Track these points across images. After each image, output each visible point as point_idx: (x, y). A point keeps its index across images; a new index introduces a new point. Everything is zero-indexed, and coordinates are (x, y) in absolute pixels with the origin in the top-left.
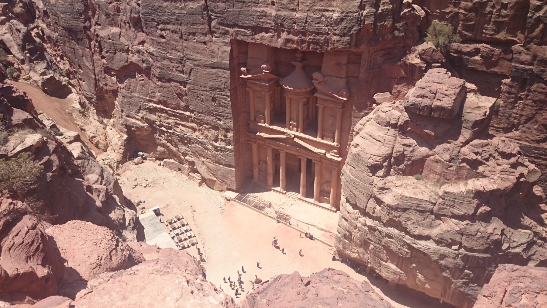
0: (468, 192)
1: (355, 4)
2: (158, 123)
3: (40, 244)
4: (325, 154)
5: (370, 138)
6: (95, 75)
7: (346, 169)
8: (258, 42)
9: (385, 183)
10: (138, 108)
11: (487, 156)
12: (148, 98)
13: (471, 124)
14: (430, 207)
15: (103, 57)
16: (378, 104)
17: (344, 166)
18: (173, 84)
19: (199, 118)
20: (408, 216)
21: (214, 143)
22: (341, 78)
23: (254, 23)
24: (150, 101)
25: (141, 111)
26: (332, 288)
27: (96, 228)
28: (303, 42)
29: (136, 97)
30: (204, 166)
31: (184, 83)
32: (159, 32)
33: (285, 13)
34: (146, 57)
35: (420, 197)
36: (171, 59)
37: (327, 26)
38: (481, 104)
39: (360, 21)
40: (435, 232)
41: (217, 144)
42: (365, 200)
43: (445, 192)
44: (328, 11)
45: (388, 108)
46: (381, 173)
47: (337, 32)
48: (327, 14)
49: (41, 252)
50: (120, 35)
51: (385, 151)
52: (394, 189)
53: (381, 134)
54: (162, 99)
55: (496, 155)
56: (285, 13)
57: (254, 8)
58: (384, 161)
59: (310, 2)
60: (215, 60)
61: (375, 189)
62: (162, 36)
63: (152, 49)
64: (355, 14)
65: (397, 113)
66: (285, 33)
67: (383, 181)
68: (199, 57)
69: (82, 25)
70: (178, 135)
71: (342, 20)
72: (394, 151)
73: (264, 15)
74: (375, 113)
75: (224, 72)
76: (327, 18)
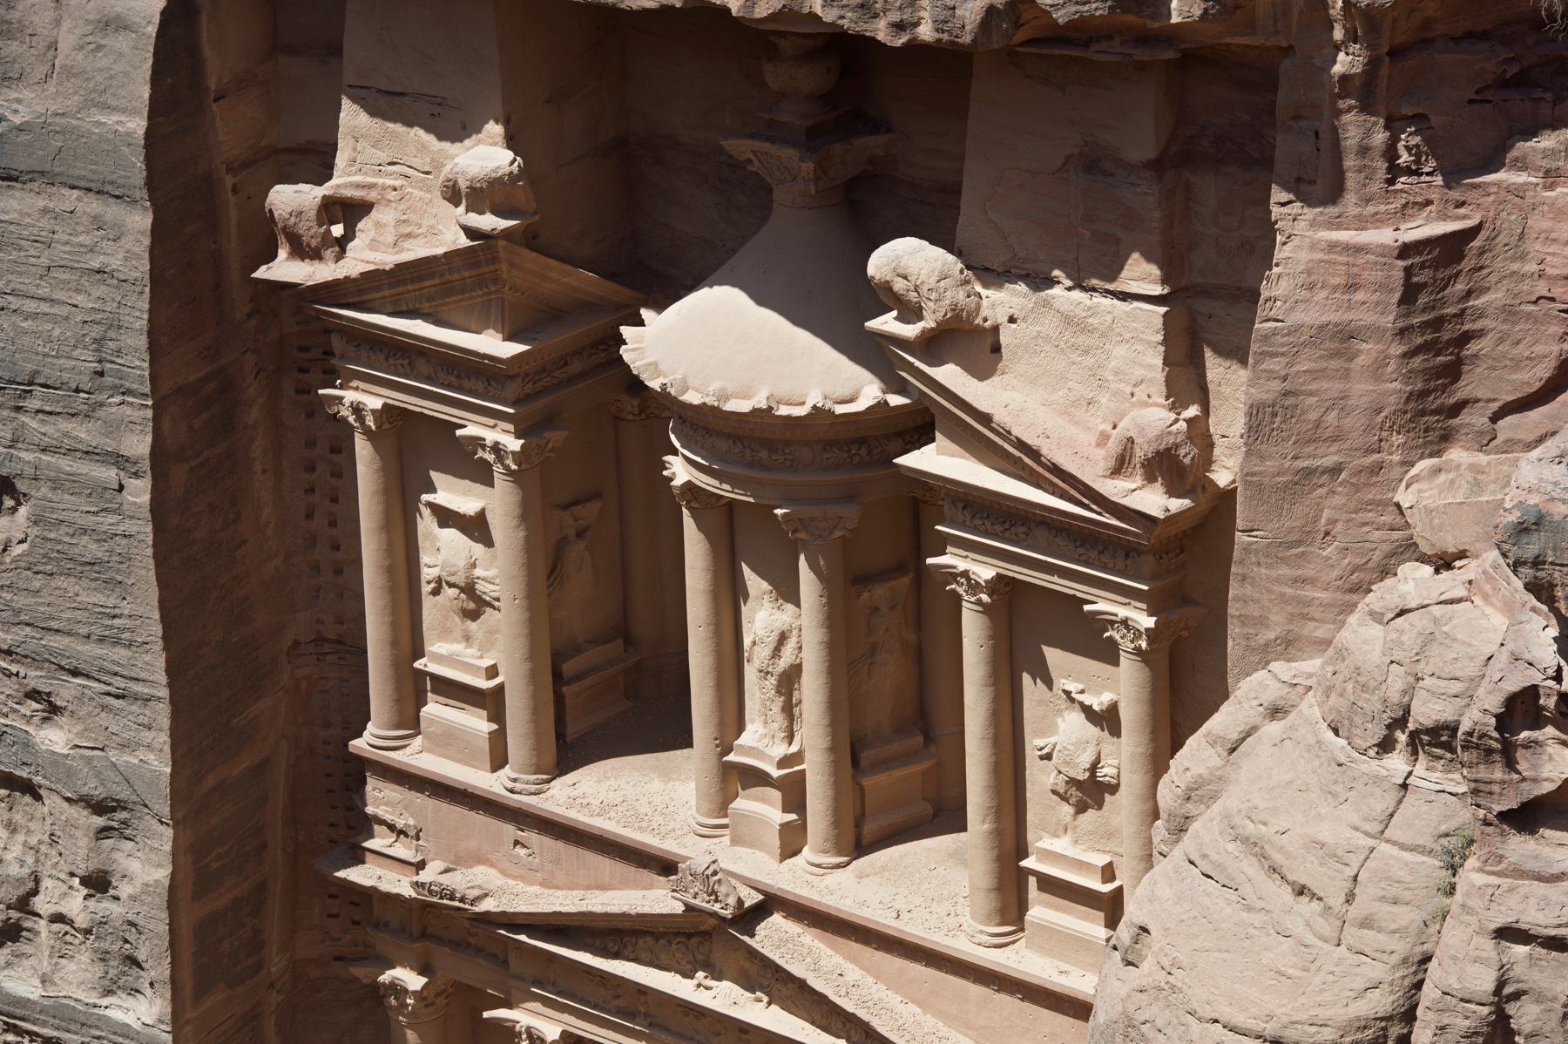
5: (1251, 868)
22: (1125, 297)
72: (1429, 994)
75: (98, 223)
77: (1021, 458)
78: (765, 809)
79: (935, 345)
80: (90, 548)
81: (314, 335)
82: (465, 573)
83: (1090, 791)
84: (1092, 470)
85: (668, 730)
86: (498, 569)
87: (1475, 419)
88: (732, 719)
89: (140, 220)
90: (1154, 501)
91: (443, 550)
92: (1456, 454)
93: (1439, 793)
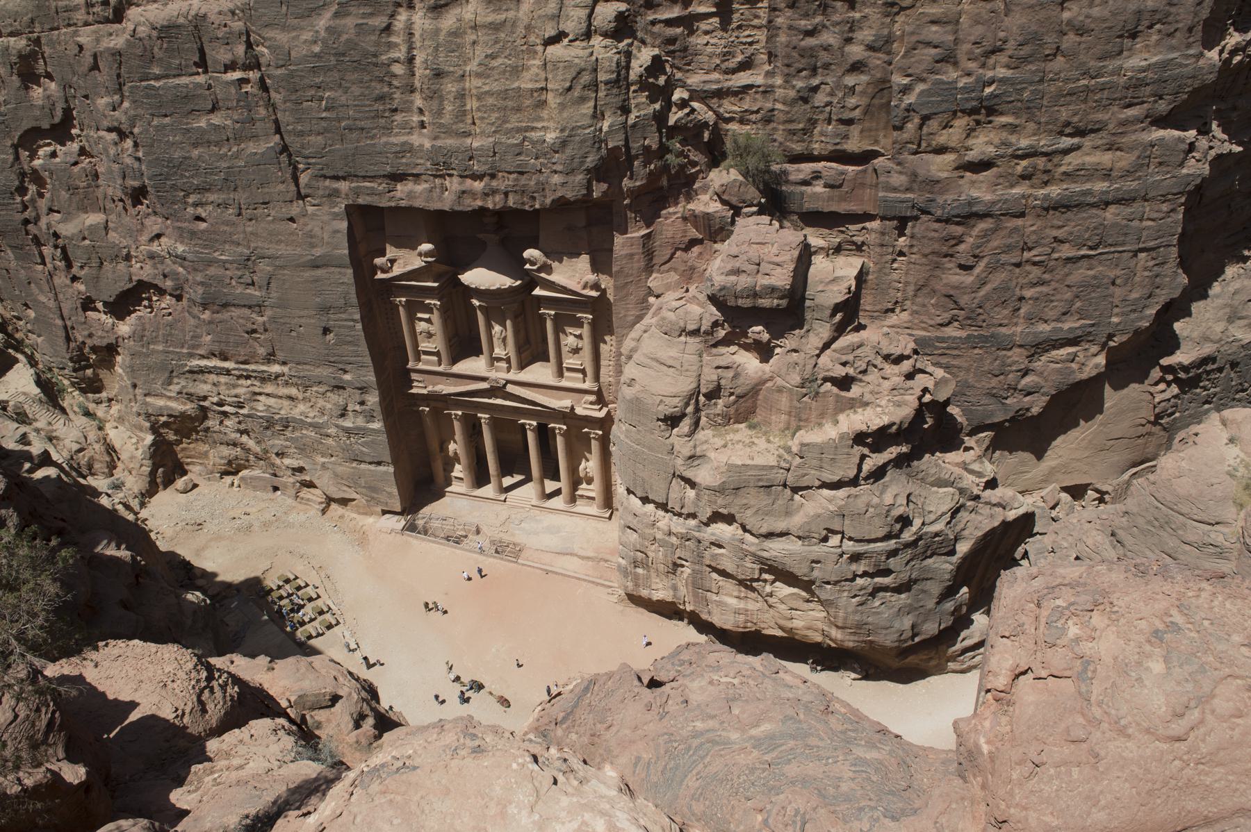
0: (842, 436)
1: (584, 111)
2: (215, 400)
3: (53, 713)
4: (572, 408)
5: (655, 364)
6: (63, 319)
7: (617, 431)
8: (403, 203)
9: (695, 447)
10: (167, 375)
11: (864, 366)
12: (185, 351)
13: (828, 312)
14: (780, 476)
15: (74, 279)
16: (658, 297)
17: (614, 427)
18: (236, 312)
19: (302, 374)
20: (745, 501)
21: (341, 422)
23: (388, 169)
24: (191, 355)
25: (176, 380)
26: (711, 683)
27: (154, 650)
28: (494, 192)
29: (158, 352)
30: (328, 474)
31: (259, 307)
32: (190, 210)
33: (450, 142)
34: (169, 265)
35: (759, 461)
36: (225, 262)
37: (537, 158)
38: (839, 273)
39: (598, 141)
40: (795, 522)
41: (348, 424)
42: (664, 486)
43: (802, 445)
44: (533, 129)
45: (680, 302)
46: (685, 426)
47: (559, 168)
48: (534, 135)
49: (60, 731)
50: (106, 228)
51: (686, 385)
52: (712, 455)
53: (673, 353)
54: (216, 348)
55: (878, 361)
56: (450, 142)
57: (384, 139)
58: (687, 404)
59: (497, 115)
60: (318, 252)
61: (679, 462)
62: (199, 218)
63: (180, 249)
64: (587, 131)
65: (696, 310)
66: (456, 180)
67: (691, 443)
68: (282, 250)
69: (20, 217)
70: (261, 417)
71: (564, 143)
72: (703, 382)
73: (407, 149)
74: (655, 314)
76: (533, 143)
77: (564, 290)
78: (504, 365)
79: (539, 270)
80: (350, 339)
81: (390, 287)
82: (428, 332)
83: (576, 351)
84: (578, 288)
85: (477, 352)
86: (436, 328)
87: (656, 267)
88: (492, 349)
89: (350, 271)
90: (594, 294)
91: (421, 326)
92: (654, 275)
93: (694, 343)
